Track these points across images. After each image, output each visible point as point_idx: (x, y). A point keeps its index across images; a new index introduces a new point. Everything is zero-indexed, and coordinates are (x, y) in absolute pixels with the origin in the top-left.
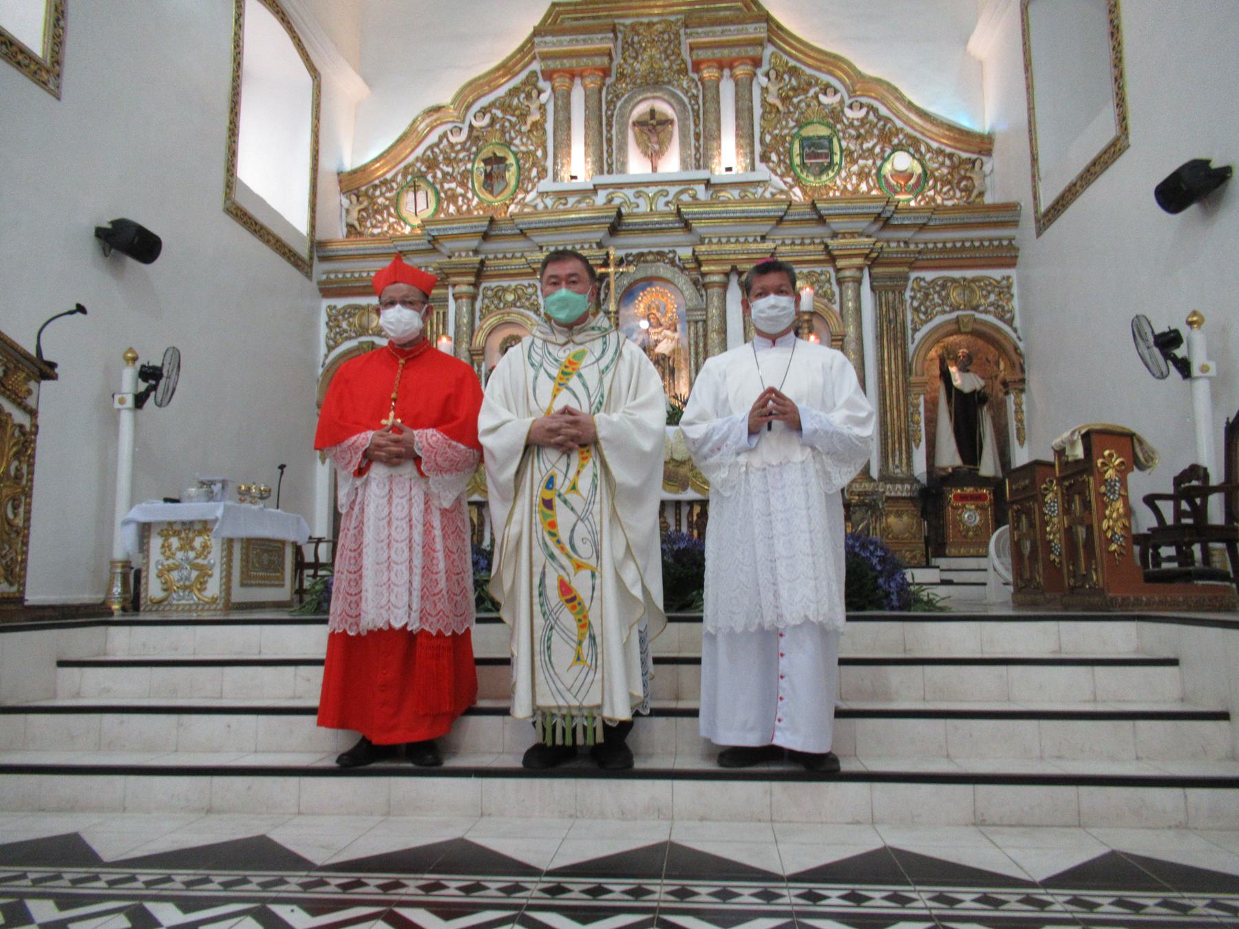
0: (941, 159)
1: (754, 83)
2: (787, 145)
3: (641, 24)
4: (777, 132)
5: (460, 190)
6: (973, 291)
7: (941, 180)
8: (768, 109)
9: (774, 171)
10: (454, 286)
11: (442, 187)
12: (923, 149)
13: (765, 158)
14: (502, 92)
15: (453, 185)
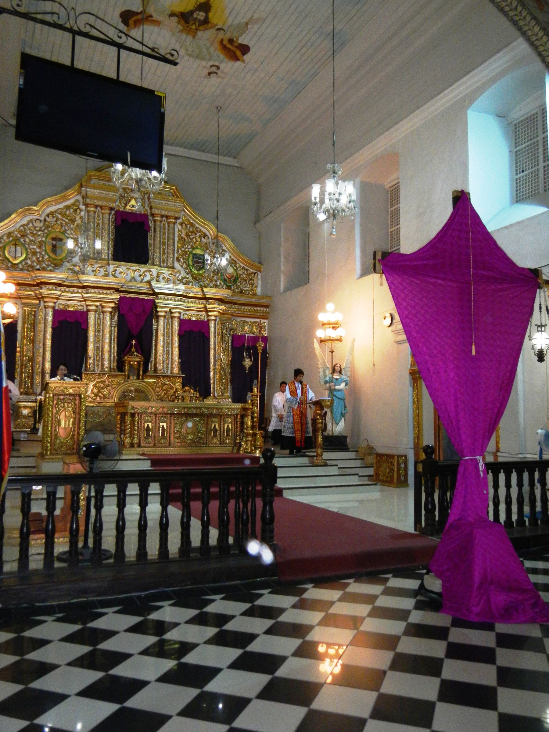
0: (244, 271)
1: (176, 226)
2: (187, 255)
3: (129, 189)
4: (183, 249)
5: (38, 250)
6: (253, 327)
7: (243, 279)
8: (181, 239)
9: (182, 266)
10: (45, 302)
11: (29, 246)
12: (237, 266)
13: (178, 260)
14: (61, 206)
15: (35, 247)
